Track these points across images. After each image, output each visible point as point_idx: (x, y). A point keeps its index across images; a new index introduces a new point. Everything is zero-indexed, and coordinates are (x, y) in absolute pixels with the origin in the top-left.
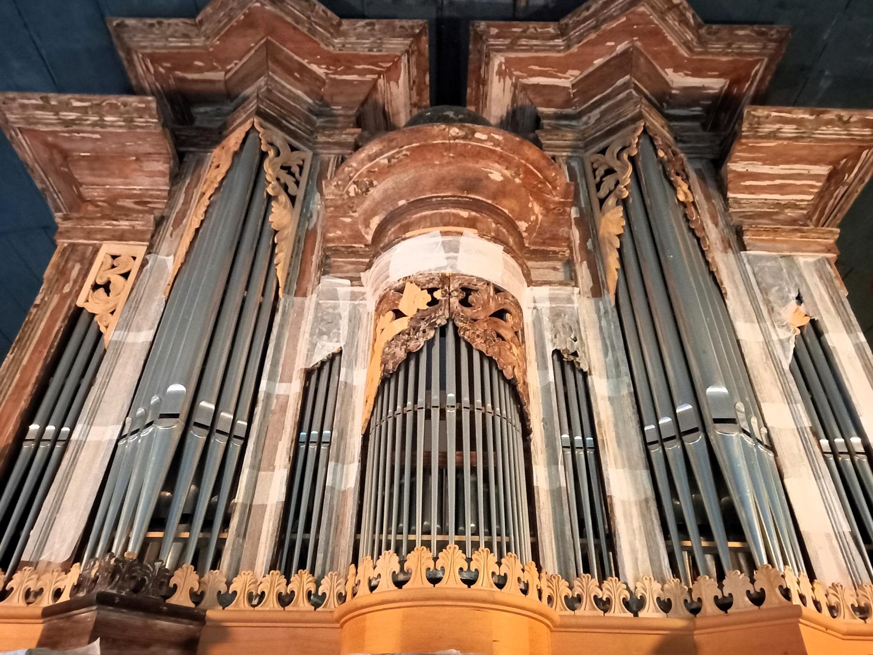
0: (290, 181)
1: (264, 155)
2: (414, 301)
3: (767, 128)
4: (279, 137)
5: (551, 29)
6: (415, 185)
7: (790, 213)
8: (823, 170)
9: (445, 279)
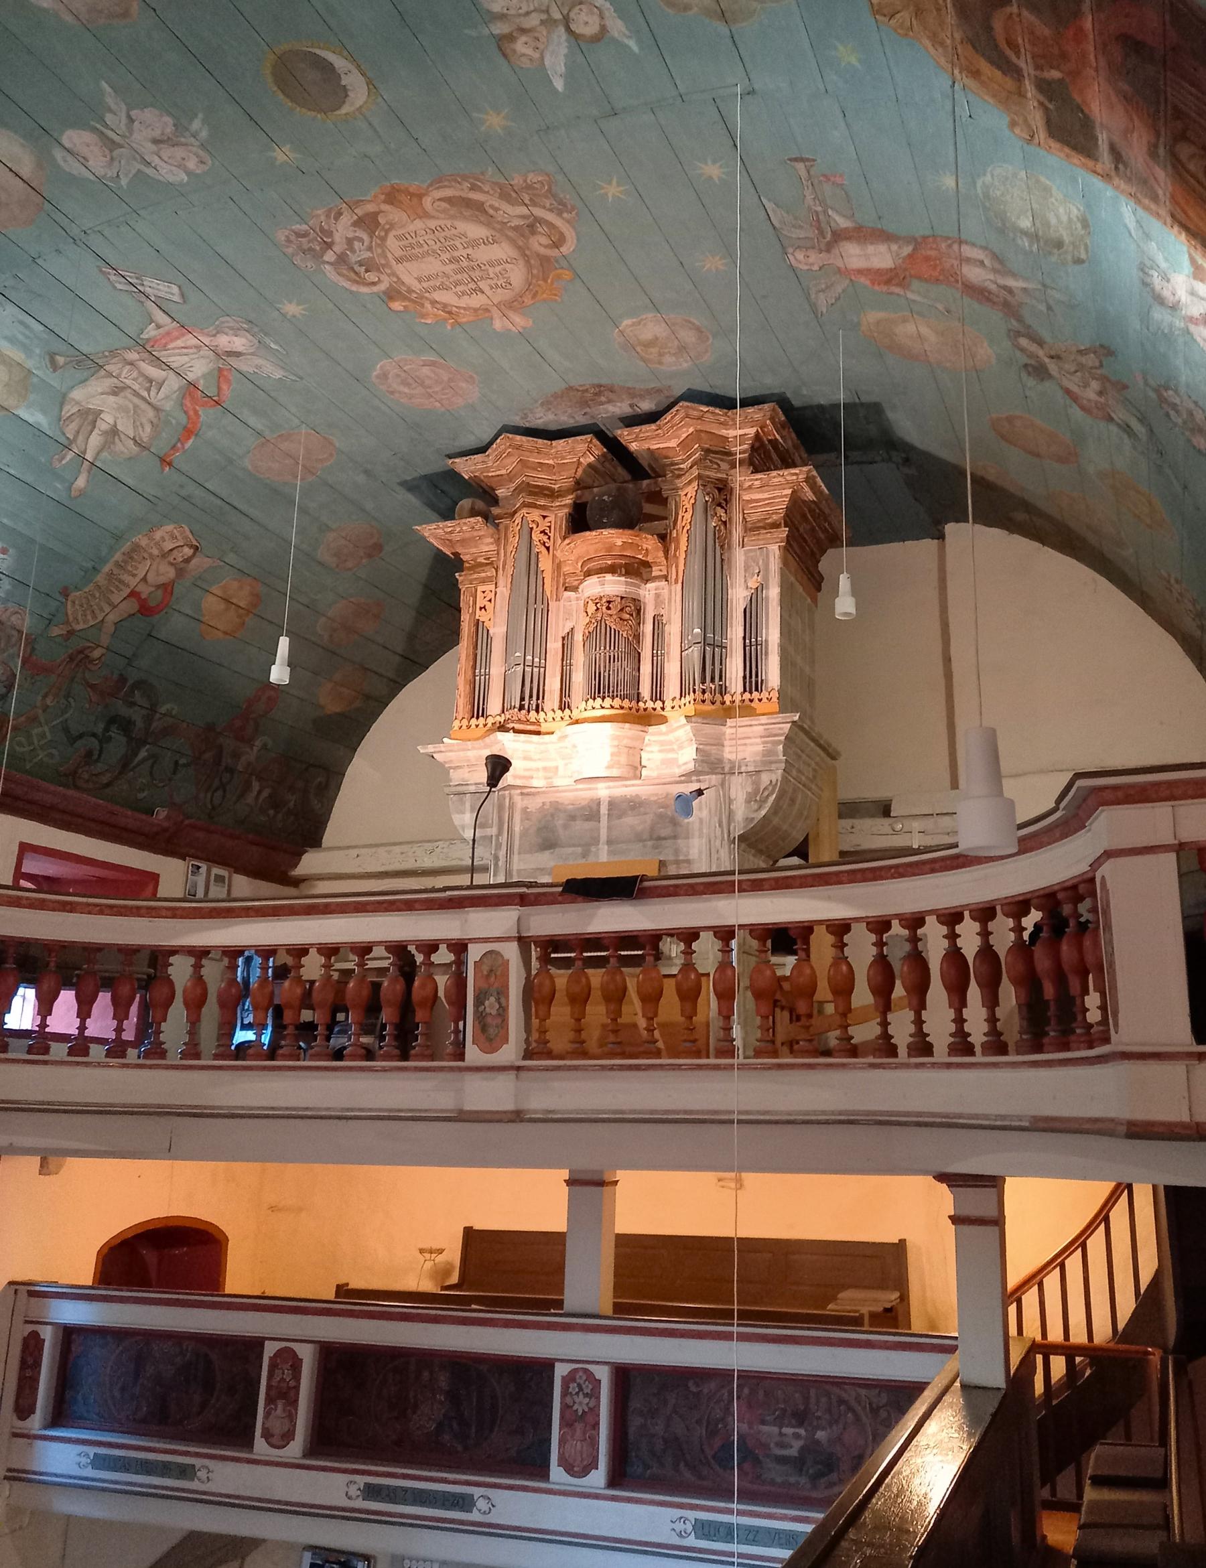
0: (545, 538)
1: (532, 529)
2: (592, 608)
3: (747, 484)
4: (535, 515)
5: (653, 426)
6: (588, 552)
7: (775, 517)
8: (789, 491)
9: (601, 598)
